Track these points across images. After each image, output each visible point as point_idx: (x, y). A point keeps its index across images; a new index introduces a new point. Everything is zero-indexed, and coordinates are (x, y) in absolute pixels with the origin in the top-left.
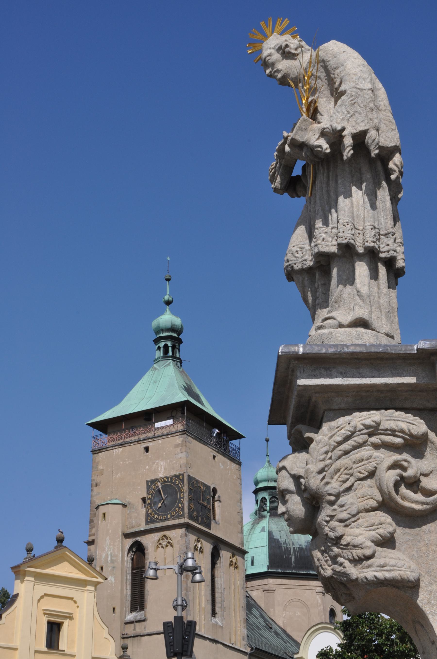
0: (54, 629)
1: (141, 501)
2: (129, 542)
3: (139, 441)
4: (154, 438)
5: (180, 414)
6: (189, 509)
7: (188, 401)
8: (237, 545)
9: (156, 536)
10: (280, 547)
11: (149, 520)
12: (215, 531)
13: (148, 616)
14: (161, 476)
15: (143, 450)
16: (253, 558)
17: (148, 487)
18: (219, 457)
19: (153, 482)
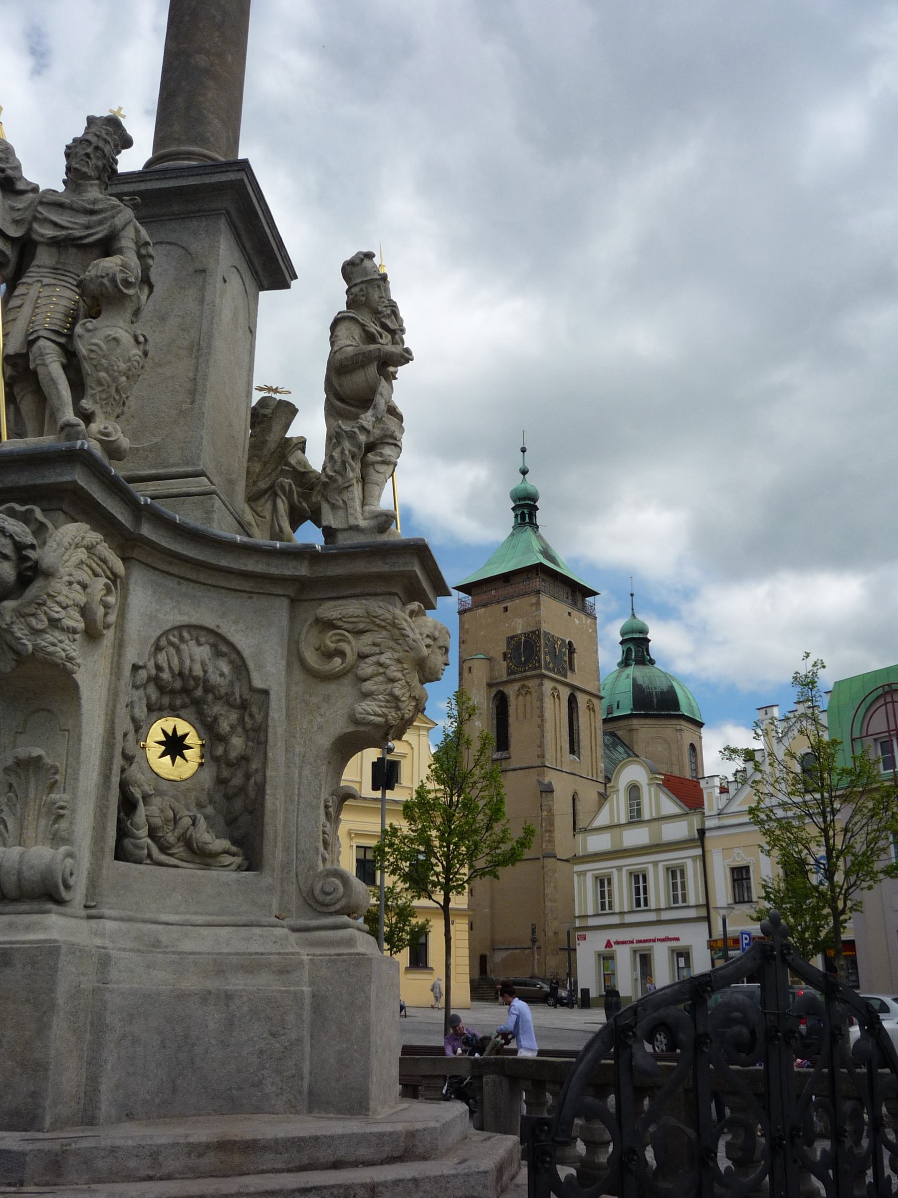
1: (502, 655)
2: (494, 691)
4: (512, 598)
5: (534, 576)
6: (545, 661)
7: (540, 565)
8: (594, 691)
9: (516, 686)
10: (643, 692)
11: (510, 672)
12: (571, 679)
13: (512, 754)
14: (519, 632)
15: (502, 610)
16: (618, 702)
17: (509, 643)
18: (575, 613)
19: (512, 638)
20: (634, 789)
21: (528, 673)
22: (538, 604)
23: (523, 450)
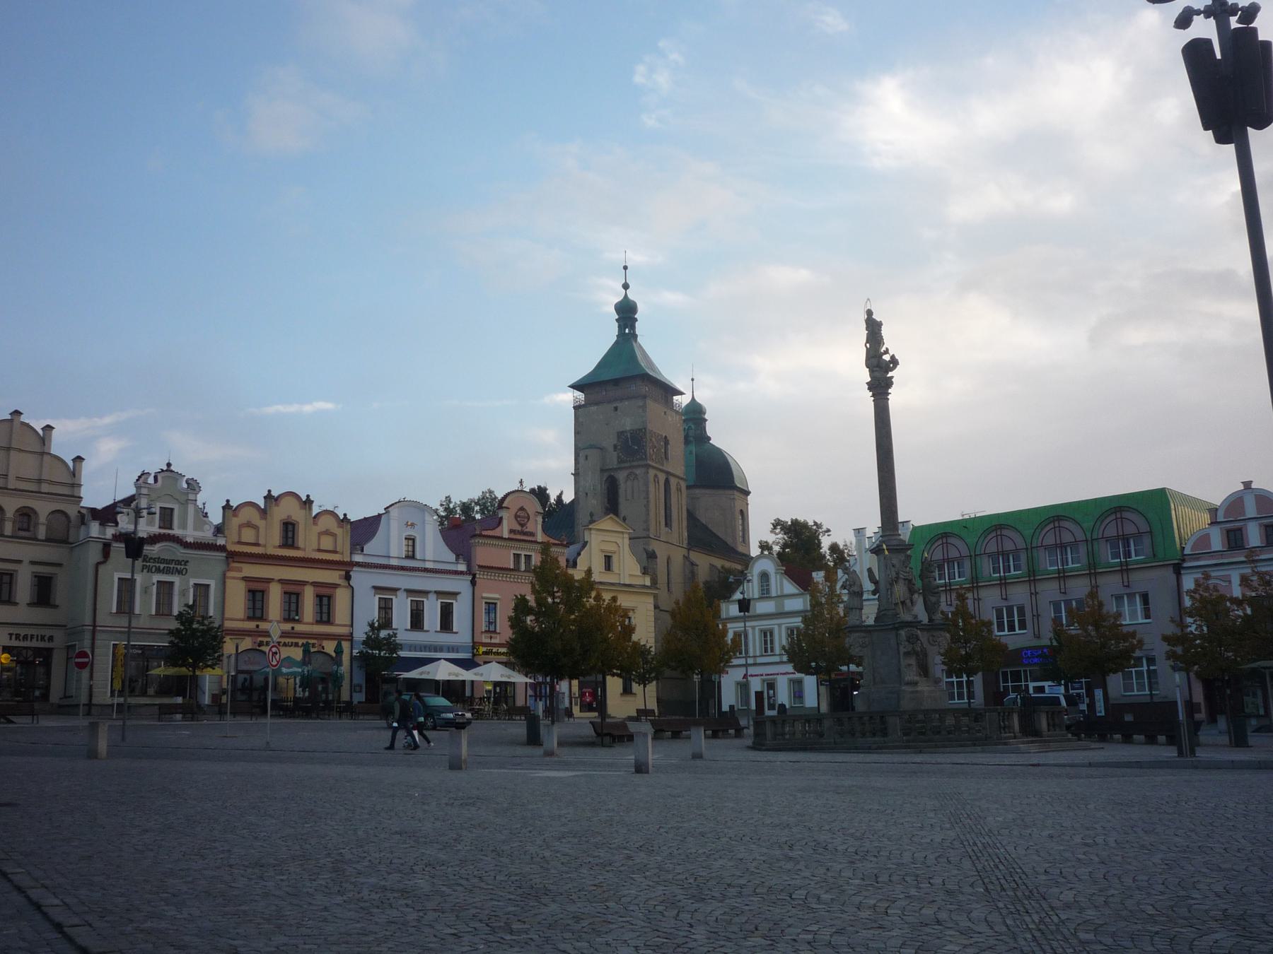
0: (608, 559)
2: (606, 475)
3: (609, 402)
4: (622, 400)
11: (620, 461)
17: (619, 437)
18: (669, 412)
20: (764, 576)
21: (635, 463)
22: (644, 407)
23: (625, 268)
